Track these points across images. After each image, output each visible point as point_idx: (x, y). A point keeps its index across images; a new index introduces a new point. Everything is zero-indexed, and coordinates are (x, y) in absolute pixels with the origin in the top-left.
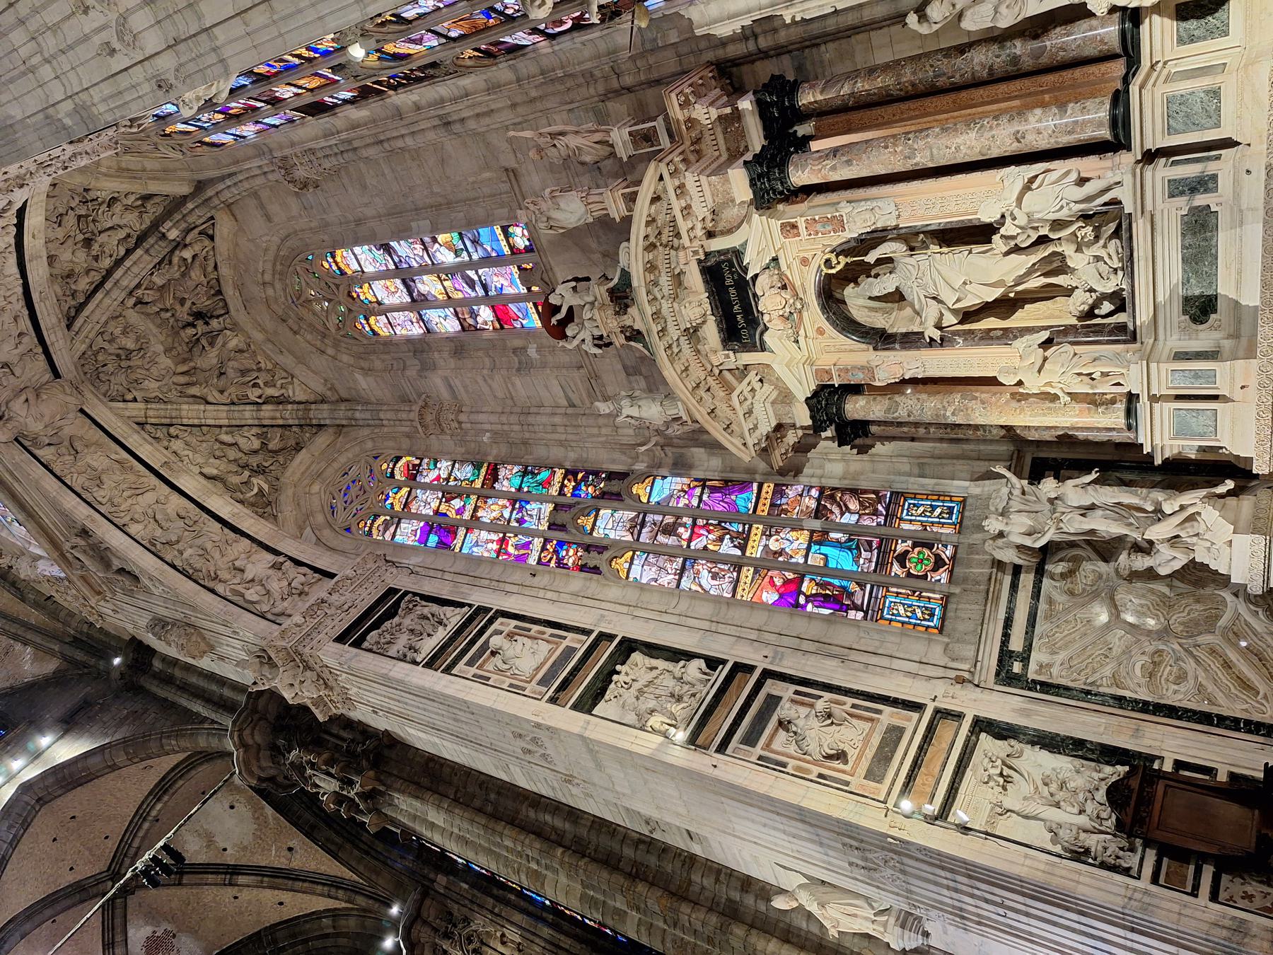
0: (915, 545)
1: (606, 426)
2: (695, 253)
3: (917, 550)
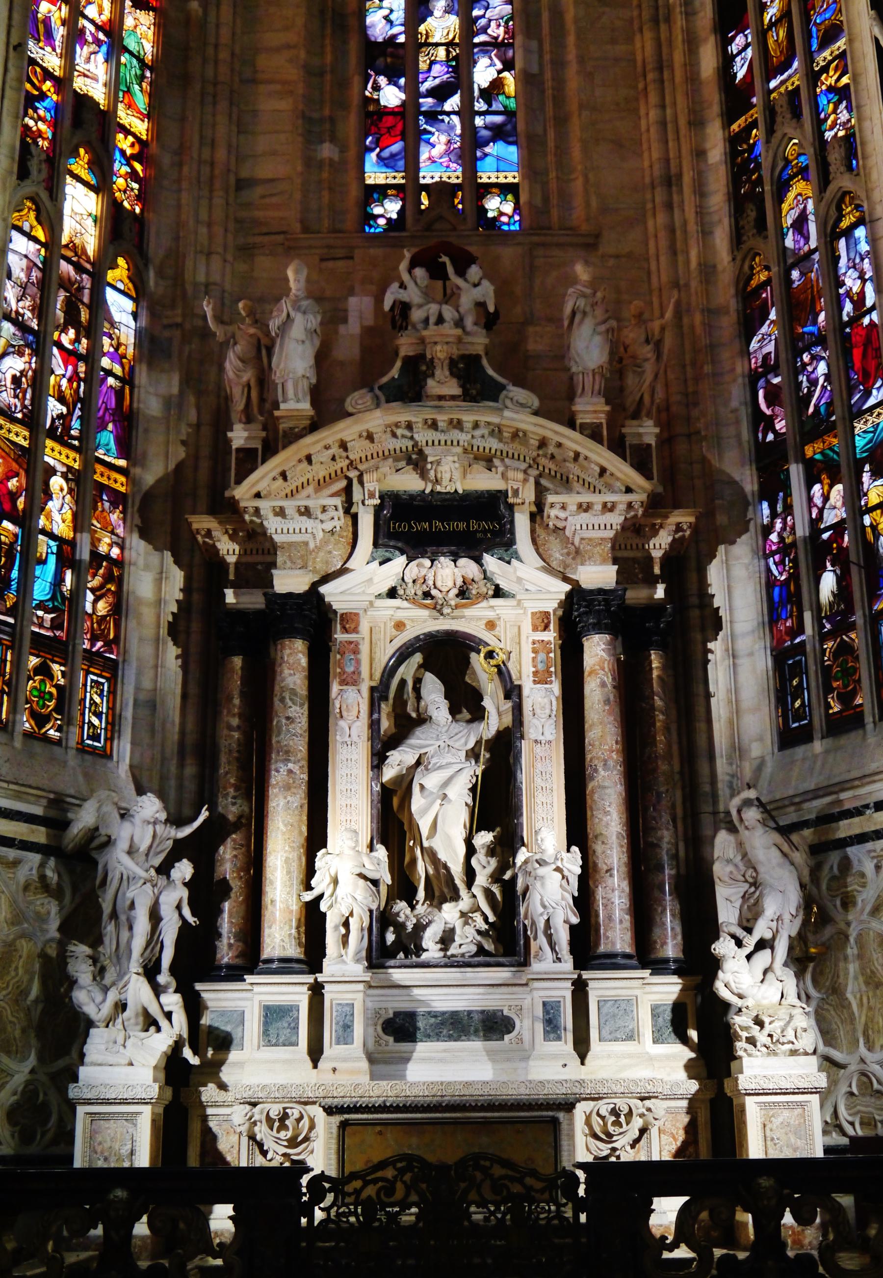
0: (57, 686)
1: (211, 237)
2: (516, 492)
3: (54, 691)
